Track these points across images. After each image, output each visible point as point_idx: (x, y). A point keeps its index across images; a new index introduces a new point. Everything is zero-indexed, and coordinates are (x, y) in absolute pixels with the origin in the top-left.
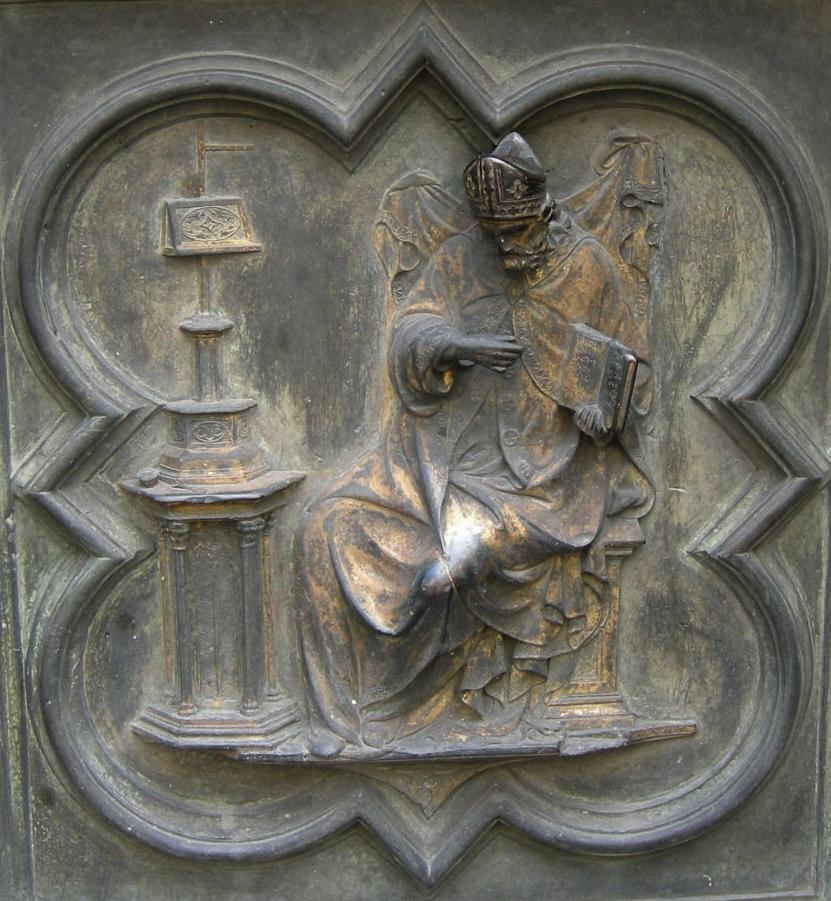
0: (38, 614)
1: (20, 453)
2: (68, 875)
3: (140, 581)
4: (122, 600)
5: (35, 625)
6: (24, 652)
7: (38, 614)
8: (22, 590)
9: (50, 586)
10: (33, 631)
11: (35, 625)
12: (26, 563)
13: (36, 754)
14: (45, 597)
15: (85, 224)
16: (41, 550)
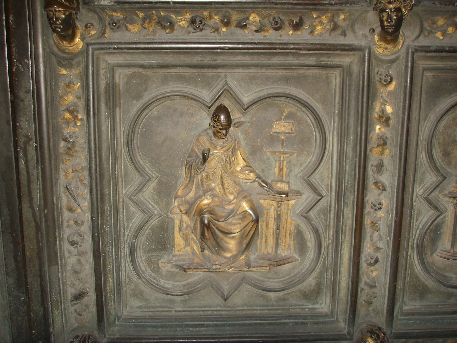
0: (418, 227)
1: (419, 187)
2: (415, 292)
3: (442, 219)
4: (437, 224)
5: (417, 229)
6: (413, 236)
7: (418, 227)
8: (415, 221)
9: (422, 220)
10: (416, 231)
11: (417, 229)
12: (417, 214)
13: (412, 262)
14: (420, 223)
15: (441, 131)
16: (420, 211)
